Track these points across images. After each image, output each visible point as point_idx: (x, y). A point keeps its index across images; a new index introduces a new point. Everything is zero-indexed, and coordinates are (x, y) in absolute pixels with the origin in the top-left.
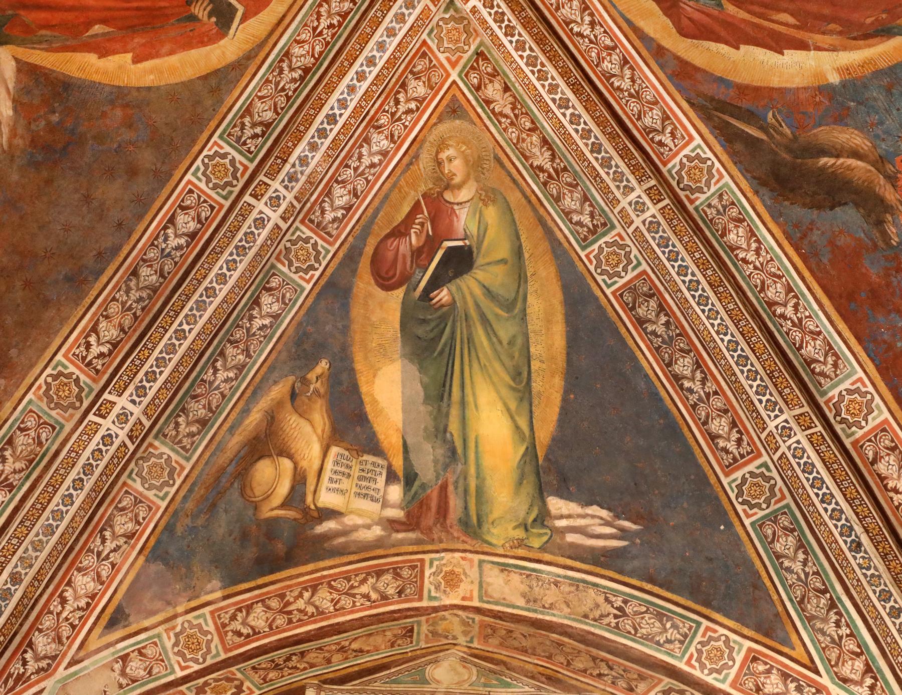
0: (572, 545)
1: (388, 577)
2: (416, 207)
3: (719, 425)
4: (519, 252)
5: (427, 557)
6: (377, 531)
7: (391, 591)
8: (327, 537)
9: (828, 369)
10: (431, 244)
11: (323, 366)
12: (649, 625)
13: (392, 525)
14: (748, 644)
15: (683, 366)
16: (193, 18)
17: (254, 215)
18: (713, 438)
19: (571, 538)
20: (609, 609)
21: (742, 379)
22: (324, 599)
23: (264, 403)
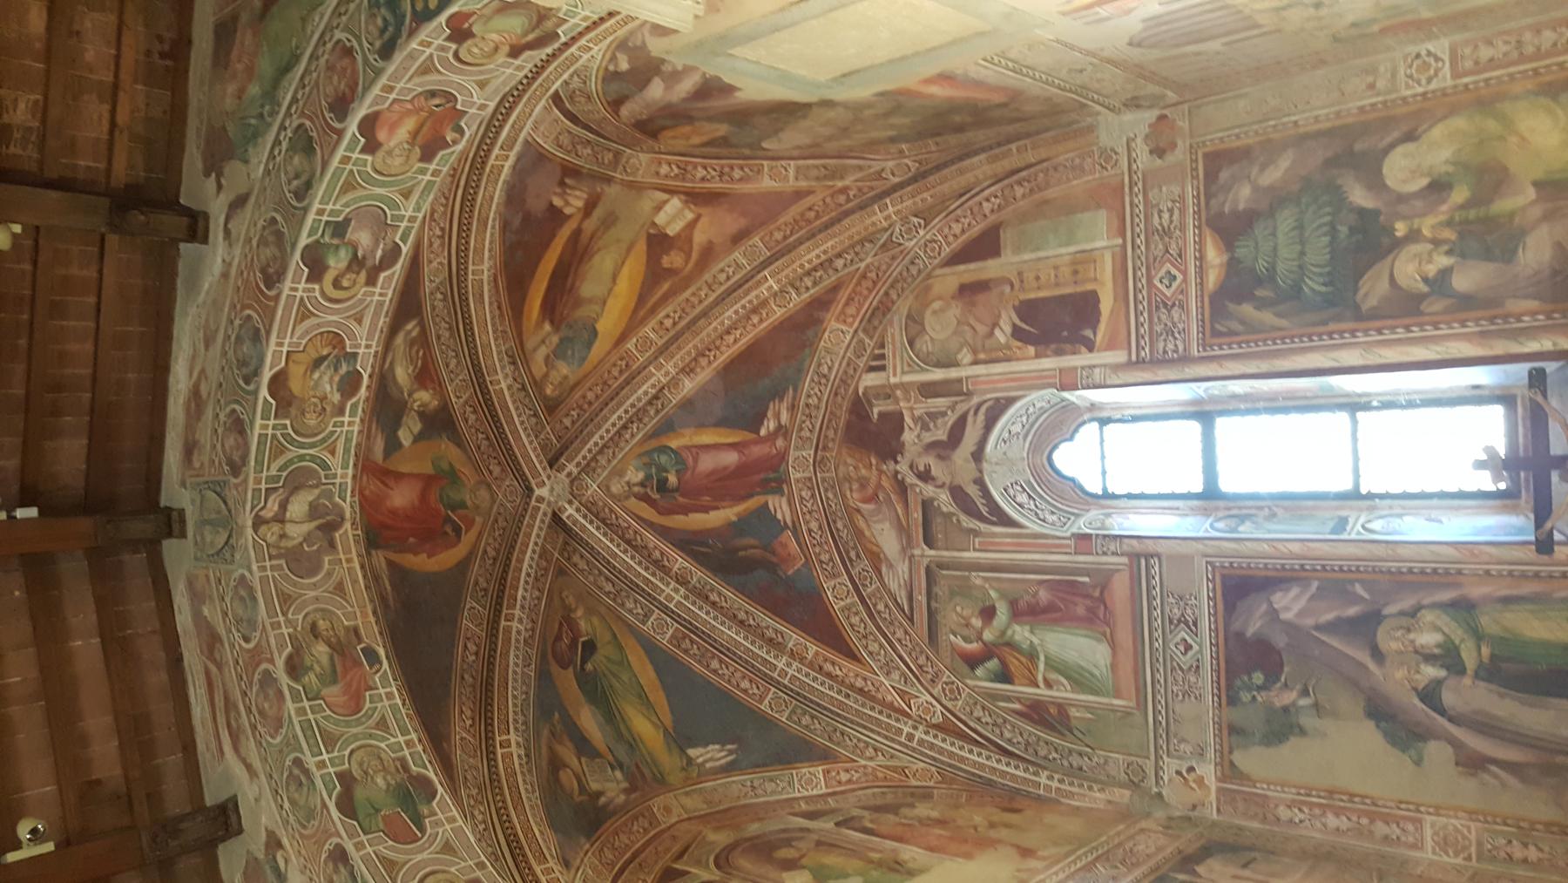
0: (711, 768)
1: (641, 819)
2: (561, 624)
3: (745, 684)
4: (614, 635)
5: (650, 803)
6: (622, 797)
7: (646, 825)
8: (606, 805)
9: (780, 639)
10: (574, 641)
11: (557, 715)
12: (770, 786)
13: (626, 791)
14: (820, 768)
15: (715, 664)
16: (446, 533)
17: (514, 630)
18: (745, 691)
19: (708, 765)
20: (744, 790)
21: (756, 651)
22: (624, 838)
23: (544, 741)
